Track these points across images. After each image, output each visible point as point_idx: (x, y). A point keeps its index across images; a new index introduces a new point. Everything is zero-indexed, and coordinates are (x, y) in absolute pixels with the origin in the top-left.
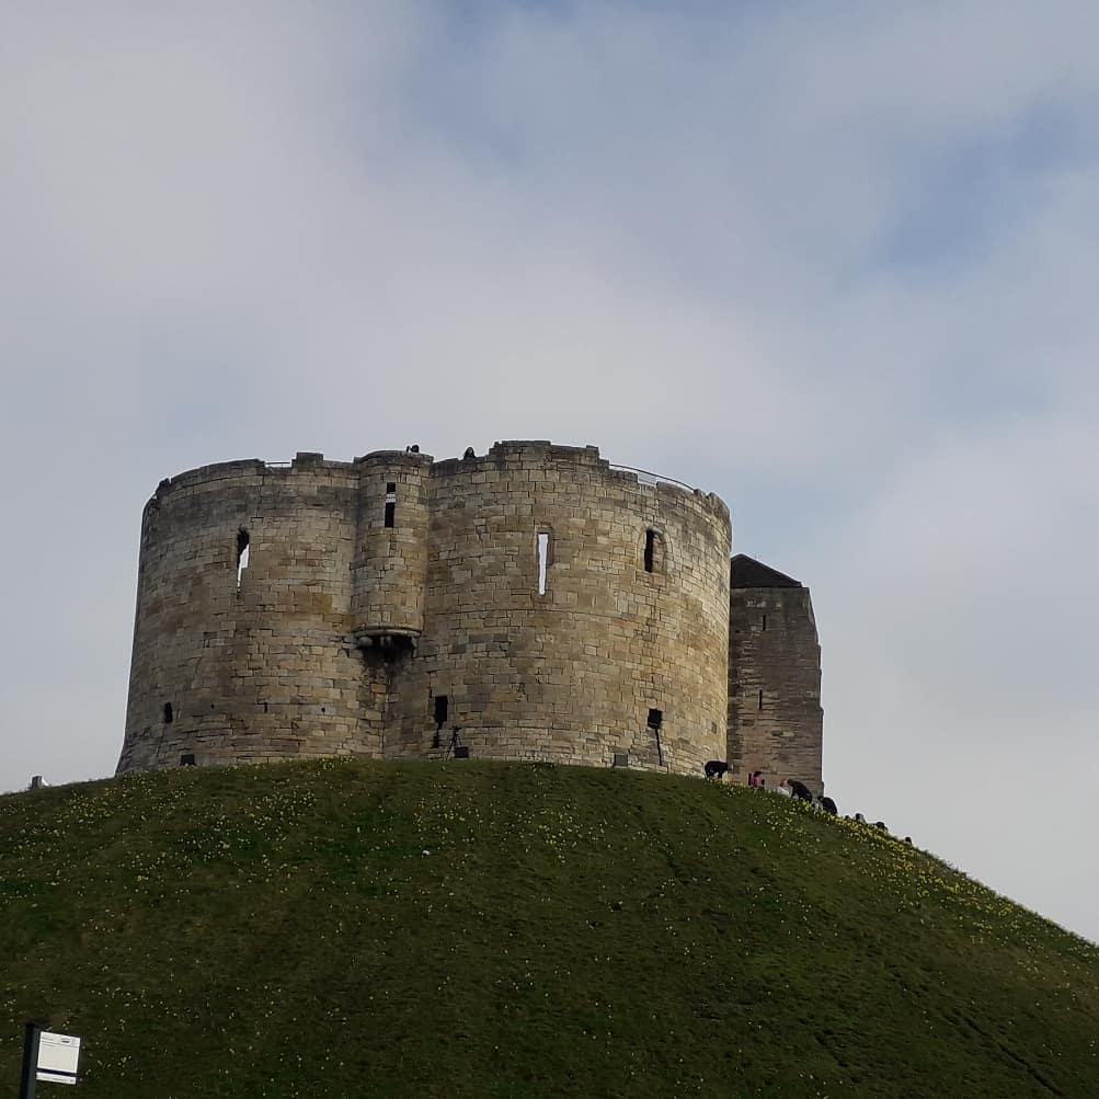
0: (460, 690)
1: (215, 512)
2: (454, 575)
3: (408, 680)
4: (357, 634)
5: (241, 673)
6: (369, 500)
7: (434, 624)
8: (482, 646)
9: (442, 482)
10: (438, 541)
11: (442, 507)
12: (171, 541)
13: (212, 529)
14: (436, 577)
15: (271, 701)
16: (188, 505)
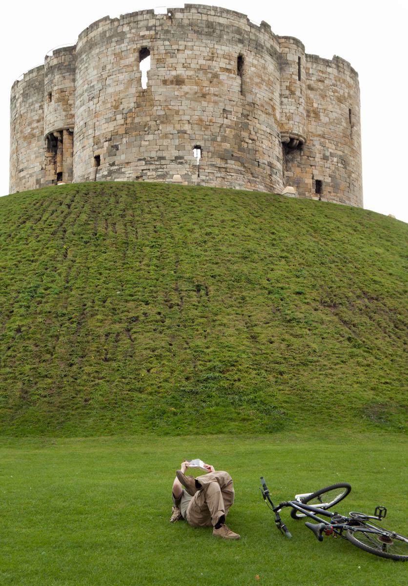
0: (328, 180)
1: (225, 37)
2: (321, 118)
3: (298, 166)
4: (282, 134)
5: (247, 140)
6: (289, 62)
7: (312, 140)
8: (335, 159)
9: (312, 65)
10: (312, 96)
11: (313, 78)
12: (190, 44)
13: (224, 48)
14: (312, 115)
15: (261, 161)
16: (204, 26)
